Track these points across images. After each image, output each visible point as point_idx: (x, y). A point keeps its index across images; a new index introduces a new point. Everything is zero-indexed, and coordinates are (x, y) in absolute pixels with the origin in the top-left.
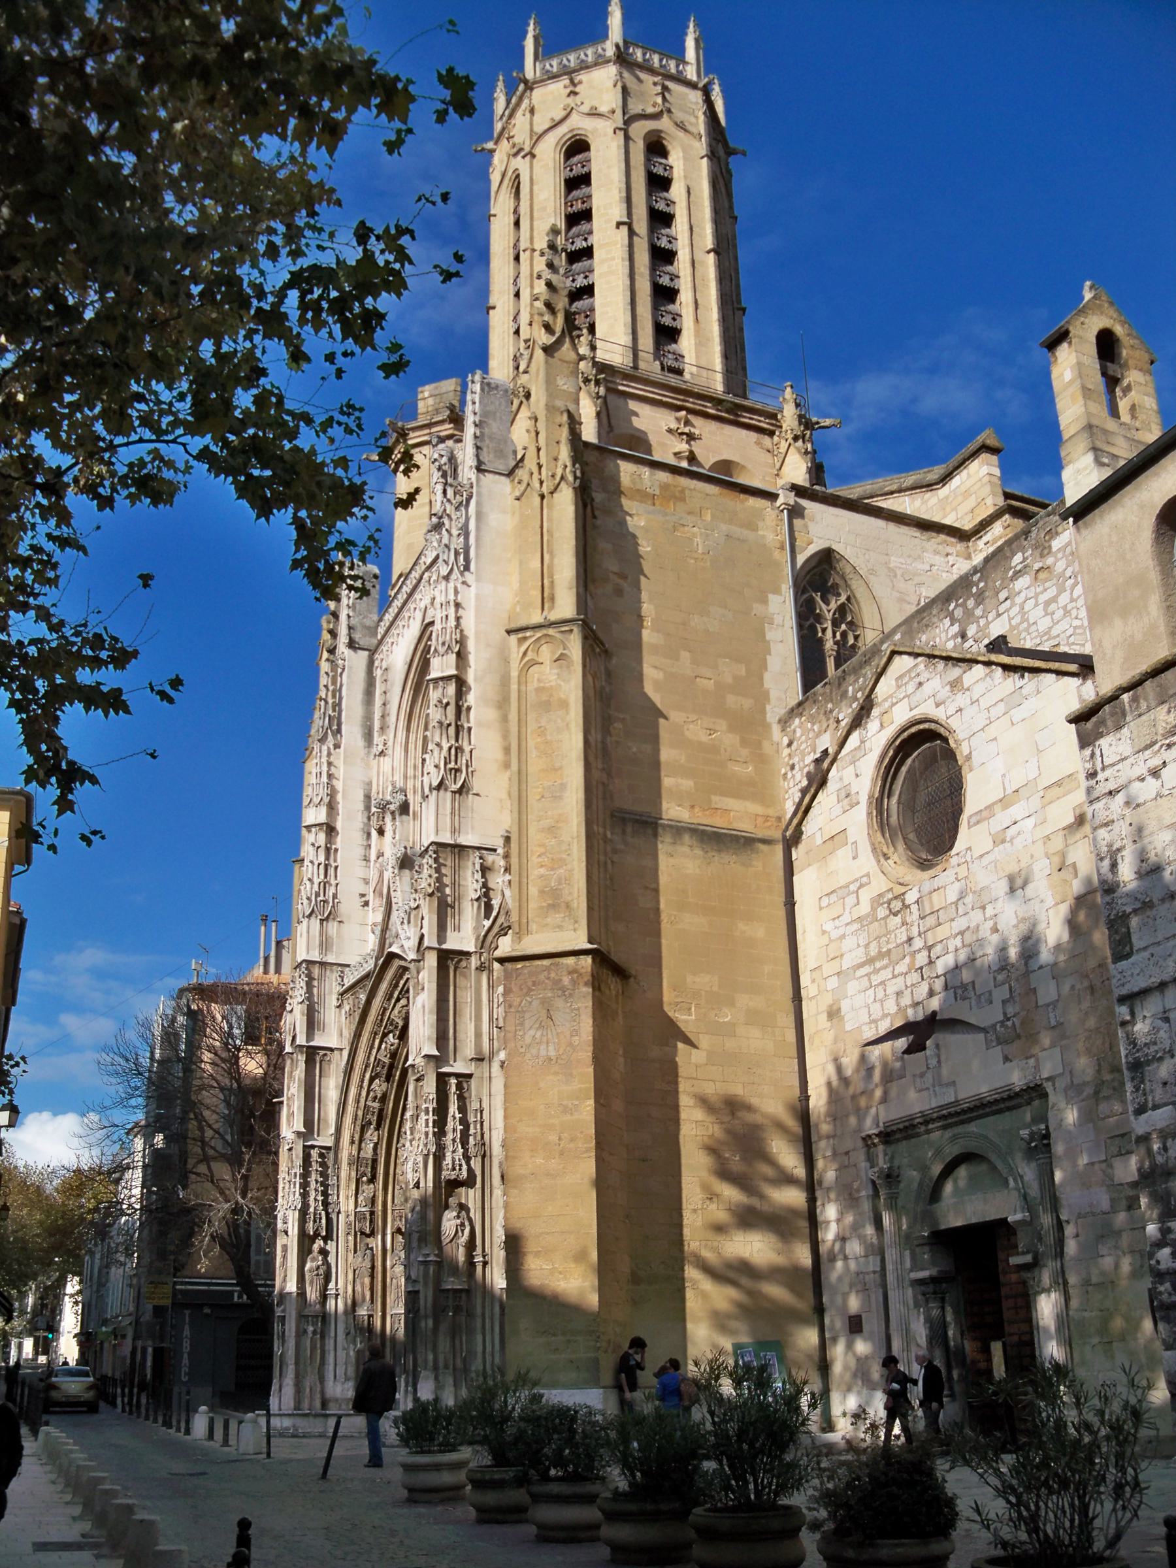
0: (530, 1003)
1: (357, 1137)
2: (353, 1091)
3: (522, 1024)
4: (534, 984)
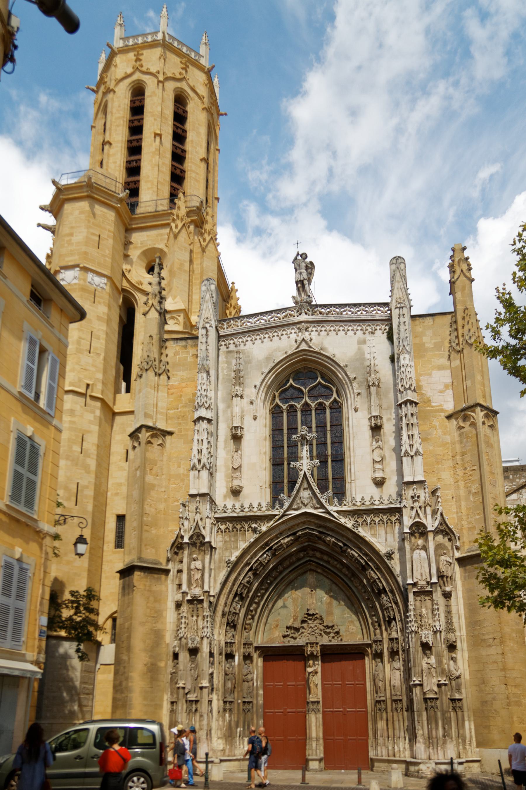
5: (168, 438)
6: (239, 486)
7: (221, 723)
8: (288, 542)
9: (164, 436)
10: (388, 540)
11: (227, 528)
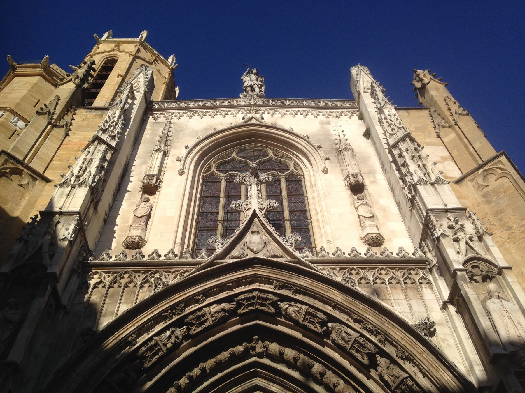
5: (39, 183)
6: (140, 237)
9: (35, 179)
10: (415, 307)
11: (100, 282)
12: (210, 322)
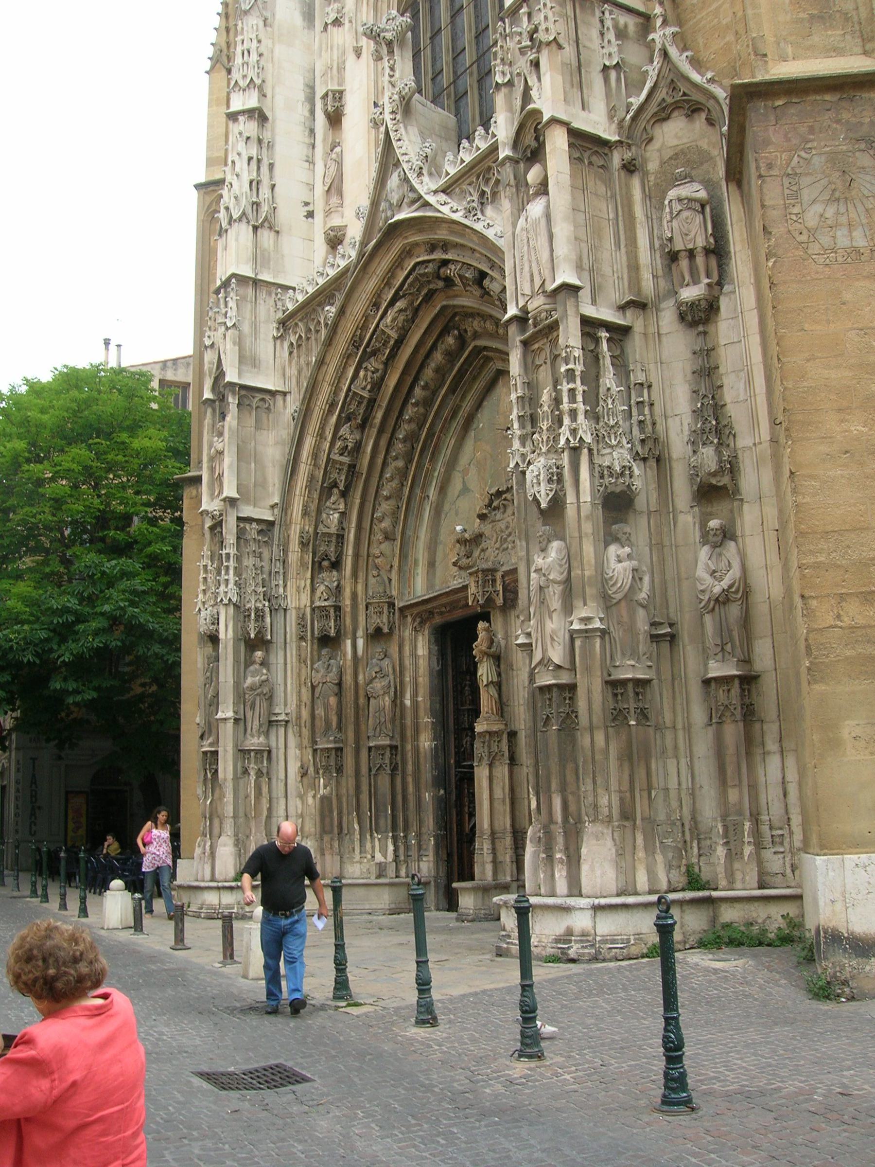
0: (808, 161)
1: (313, 507)
2: (309, 443)
3: (796, 195)
4: (811, 130)
7: (310, 801)
8: (394, 320)
12: (394, 335)
